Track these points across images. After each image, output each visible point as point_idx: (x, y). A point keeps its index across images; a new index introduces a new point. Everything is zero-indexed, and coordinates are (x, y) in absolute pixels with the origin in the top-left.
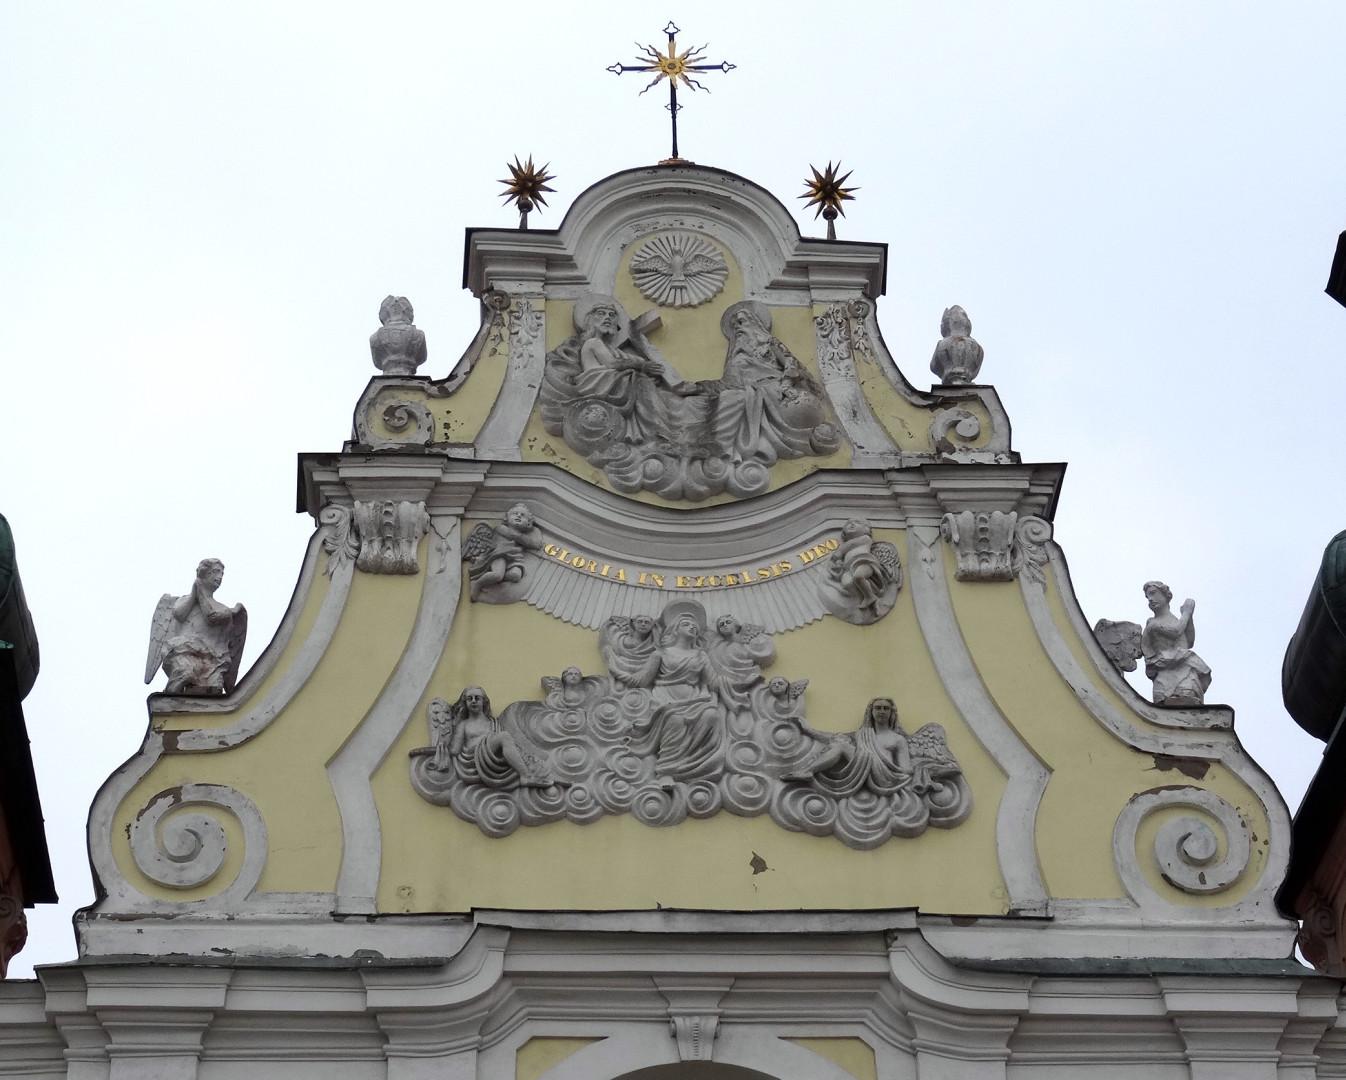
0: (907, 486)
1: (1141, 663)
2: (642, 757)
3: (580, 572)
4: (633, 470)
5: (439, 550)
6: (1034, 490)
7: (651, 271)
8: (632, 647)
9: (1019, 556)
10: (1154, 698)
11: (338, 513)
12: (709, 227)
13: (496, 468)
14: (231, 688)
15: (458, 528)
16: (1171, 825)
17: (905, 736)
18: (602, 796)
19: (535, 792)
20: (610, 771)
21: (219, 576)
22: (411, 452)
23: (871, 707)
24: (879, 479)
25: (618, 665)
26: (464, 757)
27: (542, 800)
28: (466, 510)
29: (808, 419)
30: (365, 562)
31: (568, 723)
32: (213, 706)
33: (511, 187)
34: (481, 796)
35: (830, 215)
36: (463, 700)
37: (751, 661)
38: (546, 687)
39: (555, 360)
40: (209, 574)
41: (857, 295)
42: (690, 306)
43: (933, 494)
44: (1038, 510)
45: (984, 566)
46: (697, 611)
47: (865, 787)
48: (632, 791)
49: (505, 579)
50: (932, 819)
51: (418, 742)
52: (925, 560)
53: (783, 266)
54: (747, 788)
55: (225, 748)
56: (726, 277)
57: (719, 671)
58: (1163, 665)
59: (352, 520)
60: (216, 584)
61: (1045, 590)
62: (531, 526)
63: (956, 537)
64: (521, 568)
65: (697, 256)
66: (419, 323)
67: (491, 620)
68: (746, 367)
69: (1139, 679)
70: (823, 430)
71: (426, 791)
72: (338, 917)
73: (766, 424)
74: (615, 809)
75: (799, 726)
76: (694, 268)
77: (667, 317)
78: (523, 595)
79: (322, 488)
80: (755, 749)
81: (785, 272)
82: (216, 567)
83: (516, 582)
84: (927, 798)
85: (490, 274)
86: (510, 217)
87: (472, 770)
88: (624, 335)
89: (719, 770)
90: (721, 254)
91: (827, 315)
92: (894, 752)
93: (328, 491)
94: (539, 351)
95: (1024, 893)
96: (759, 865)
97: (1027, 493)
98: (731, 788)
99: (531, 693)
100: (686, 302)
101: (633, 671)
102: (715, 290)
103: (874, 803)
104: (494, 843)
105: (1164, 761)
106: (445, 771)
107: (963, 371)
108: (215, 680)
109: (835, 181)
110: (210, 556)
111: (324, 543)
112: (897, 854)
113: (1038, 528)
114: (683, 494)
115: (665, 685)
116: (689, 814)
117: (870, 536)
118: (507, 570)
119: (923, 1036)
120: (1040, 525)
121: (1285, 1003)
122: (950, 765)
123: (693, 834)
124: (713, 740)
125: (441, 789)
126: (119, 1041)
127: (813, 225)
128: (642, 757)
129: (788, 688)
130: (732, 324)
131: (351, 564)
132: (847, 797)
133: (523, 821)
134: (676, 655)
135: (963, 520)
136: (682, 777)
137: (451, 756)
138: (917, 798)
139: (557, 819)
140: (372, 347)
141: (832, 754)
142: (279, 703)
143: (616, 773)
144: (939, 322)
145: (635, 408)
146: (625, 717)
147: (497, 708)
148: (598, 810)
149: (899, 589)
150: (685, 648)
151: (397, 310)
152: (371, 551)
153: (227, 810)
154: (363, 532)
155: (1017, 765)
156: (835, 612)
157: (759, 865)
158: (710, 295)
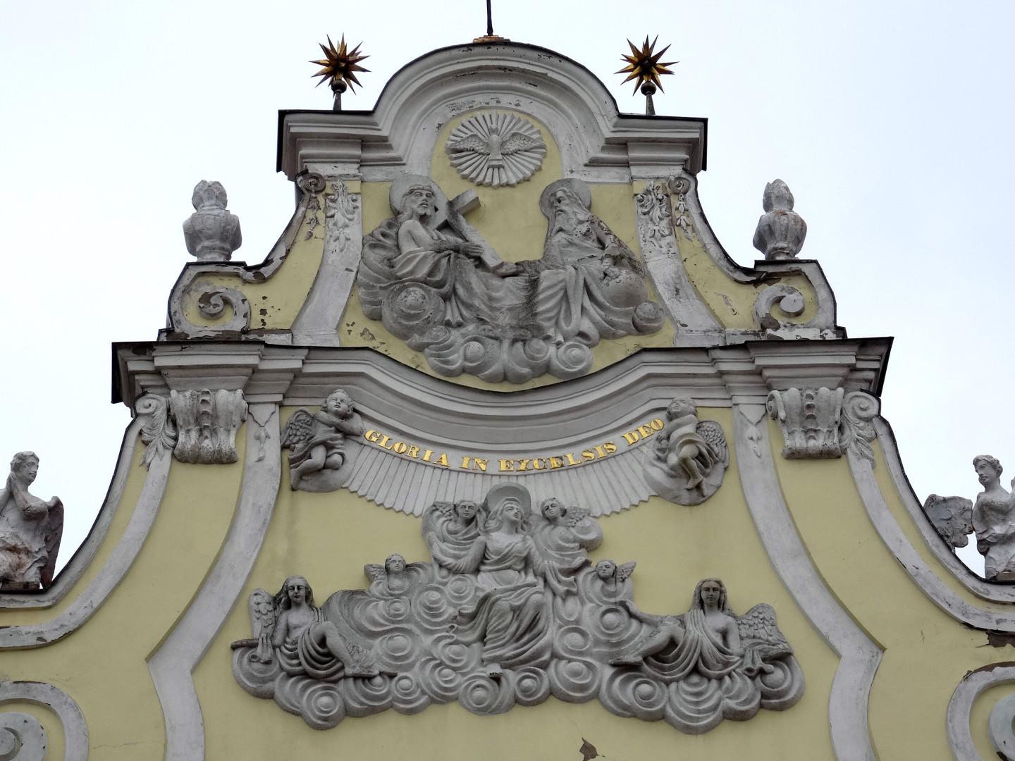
0: (732, 363)
1: (972, 539)
2: (468, 645)
3: (401, 457)
4: (453, 353)
5: (258, 438)
6: (860, 365)
7: (467, 150)
8: (456, 533)
9: (847, 432)
10: (987, 573)
11: (154, 403)
12: (527, 105)
13: (314, 354)
14: (49, 584)
15: (277, 415)
17: (735, 617)
18: (428, 685)
19: (360, 682)
20: (434, 659)
21: (33, 469)
22: (228, 340)
23: (700, 589)
24: (703, 357)
25: (442, 551)
26: (287, 649)
27: (367, 690)
28: (284, 397)
29: (630, 298)
30: (182, 453)
31: (392, 612)
32: (30, 602)
33: (323, 67)
34: (306, 688)
35: (648, 91)
36: (285, 590)
37: (577, 544)
38: (369, 575)
39: (372, 243)
40: (24, 467)
41: (677, 170)
42: (508, 185)
43: (759, 372)
44: (865, 386)
45: (812, 443)
46: (520, 494)
47: (695, 670)
48: (459, 679)
49: (325, 467)
50: (764, 701)
52: (752, 439)
53: (602, 143)
54: (576, 674)
55: (43, 645)
56: (544, 155)
57: (544, 555)
58: (994, 541)
59: (169, 410)
60: (30, 477)
61: (873, 467)
62: (351, 412)
63: (782, 415)
64: (342, 455)
65: (514, 135)
66: (233, 207)
67: (312, 508)
68: (567, 246)
69: (970, 555)
70: (645, 309)
71: (249, 684)
73: (587, 303)
74: (441, 698)
75: (627, 609)
76: (512, 147)
77: (486, 197)
78: (345, 482)
79: (137, 377)
80: (583, 633)
81: (603, 149)
82: (31, 460)
83: (337, 469)
84: (758, 679)
85: (303, 157)
86: (323, 98)
87: (295, 662)
88: (442, 216)
89: (546, 657)
90: (539, 132)
91: (648, 192)
92: (724, 634)
93: (143, 380)
94: (355, 233)
97: (853, 369)
98: (559, 674)
99: (355, 582)
100: (504, 180)
101: (457, 557)
102: (533, 168)
103: (704, 686)
104: (320, 734)
106: (268, 663)
107: (785, 246)
108: (32, 576)
109: (652, 56)
110: (24, 449)
111: (140, 433)
113: (865, 404)
114: (505, 378)
115: (490, 571)
116: (517, 701)
117: (695, 415)
118: (327, 457)
120: (867, 401)
122: (781, 646)
123: (522, 720)
124: (540, 626)
125: (264, 681)
127: (631, 101)
128: (468, 645)
129: (615, 571)
130: (551, 202)
131: (168, 454)
132: (677, 681)
133: (348, 712)
134: (501, 540)
135: (788, 398)
136: (509, 663)
137: (274, 647)
138: (748, 680)
139: (383, 709)
140: (186, 233)
141: (661, 638)
142: (97, 599)
143: (442, 661)
144: (761, 197)
145: (454, 290)
146: (450, 604)
147: (319, 597)
148: (424, 699)
149: (726, 469)
150: (510, 533)
152: (188, 440)
153: (47, 707)
154: (180, 422)
155: (850, 645)
156: (661, 494)
158: (528, 173)
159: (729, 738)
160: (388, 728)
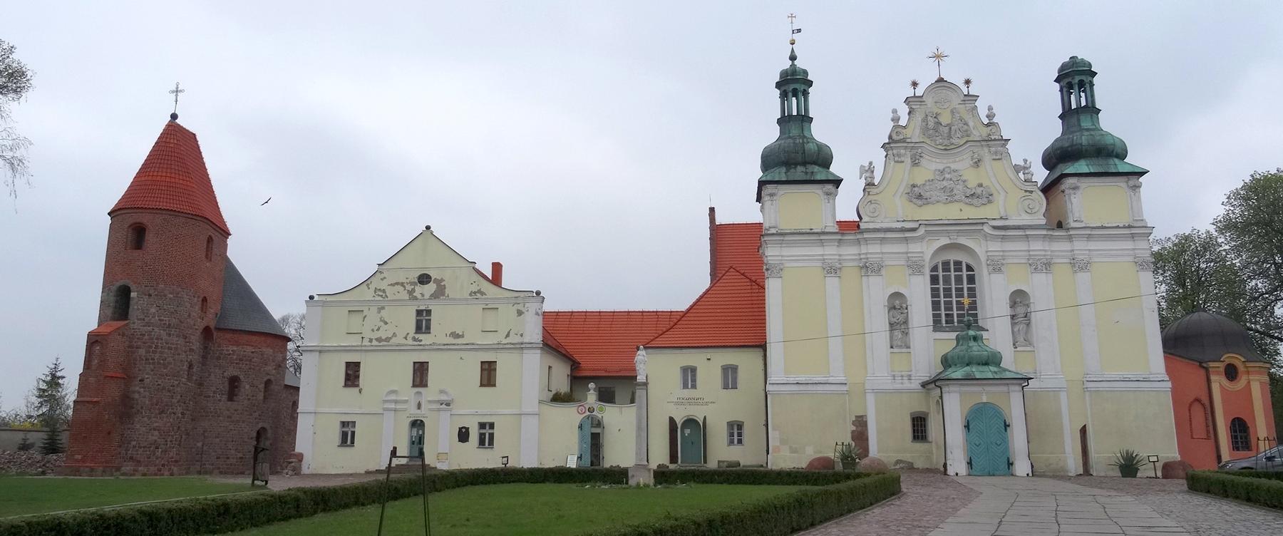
0: (983, 143)
16: (1027, 202)
29: (966, 131)
51: (906, 192)
67: (916, 169)
69: (1021, 175)
70: (969, 132)
72: (898, 221)
94: (920, 119)
95: (1003, 214)
96: (961, 210)
98: (955, 198)
105: (1026, 191)
112: (983, 208)
119: (988, 239)
121: (1044, 232)
126: (868, 242)
130: (952, 112)
134: (948, 176)
135: (993, 149)
142: (885, 186)
151: (895, 111)
152: (896, 159)
155: (1003, 193)
156: (972, 166)
157: (961, 210)
159: (983, 207)
160: (930, 206)
